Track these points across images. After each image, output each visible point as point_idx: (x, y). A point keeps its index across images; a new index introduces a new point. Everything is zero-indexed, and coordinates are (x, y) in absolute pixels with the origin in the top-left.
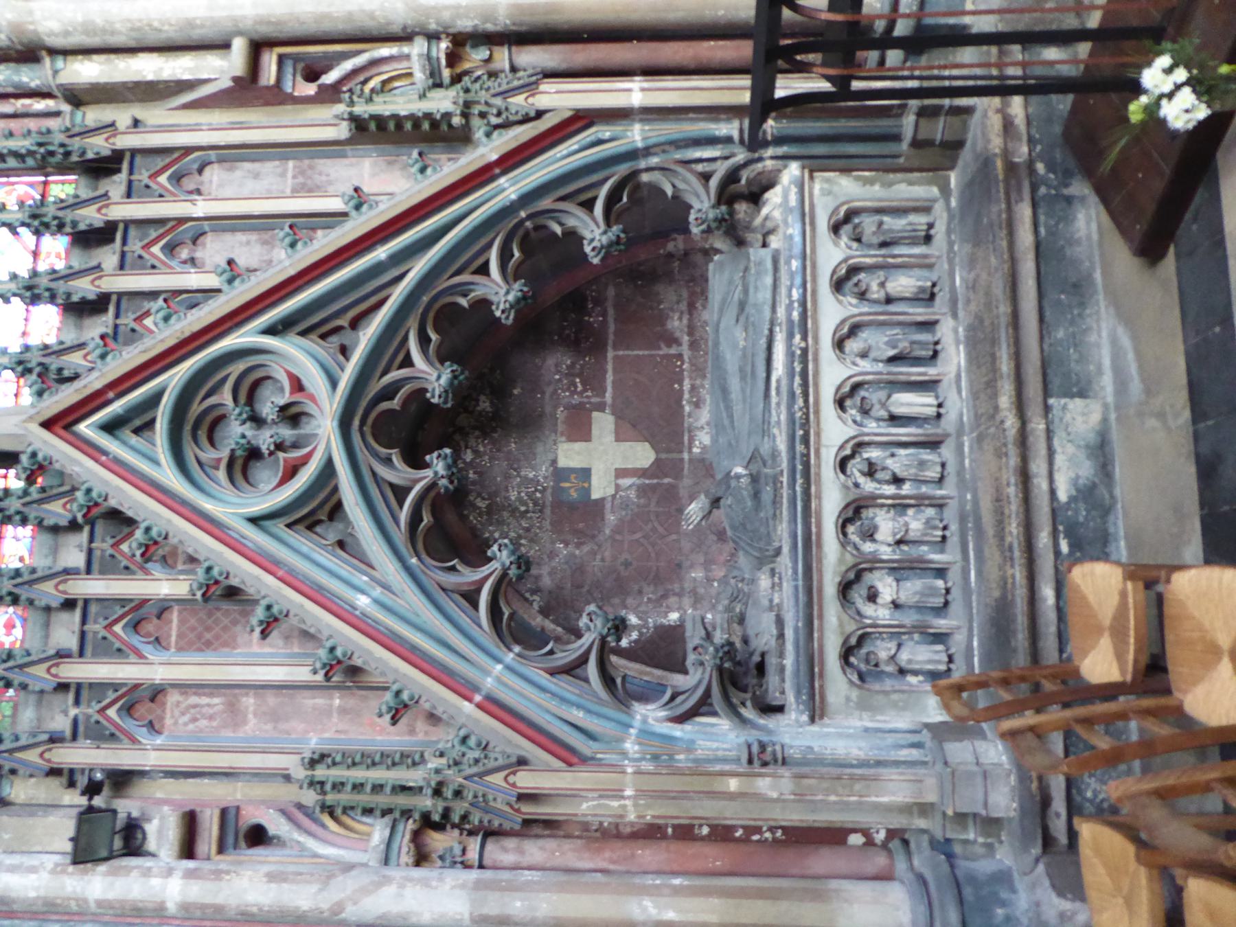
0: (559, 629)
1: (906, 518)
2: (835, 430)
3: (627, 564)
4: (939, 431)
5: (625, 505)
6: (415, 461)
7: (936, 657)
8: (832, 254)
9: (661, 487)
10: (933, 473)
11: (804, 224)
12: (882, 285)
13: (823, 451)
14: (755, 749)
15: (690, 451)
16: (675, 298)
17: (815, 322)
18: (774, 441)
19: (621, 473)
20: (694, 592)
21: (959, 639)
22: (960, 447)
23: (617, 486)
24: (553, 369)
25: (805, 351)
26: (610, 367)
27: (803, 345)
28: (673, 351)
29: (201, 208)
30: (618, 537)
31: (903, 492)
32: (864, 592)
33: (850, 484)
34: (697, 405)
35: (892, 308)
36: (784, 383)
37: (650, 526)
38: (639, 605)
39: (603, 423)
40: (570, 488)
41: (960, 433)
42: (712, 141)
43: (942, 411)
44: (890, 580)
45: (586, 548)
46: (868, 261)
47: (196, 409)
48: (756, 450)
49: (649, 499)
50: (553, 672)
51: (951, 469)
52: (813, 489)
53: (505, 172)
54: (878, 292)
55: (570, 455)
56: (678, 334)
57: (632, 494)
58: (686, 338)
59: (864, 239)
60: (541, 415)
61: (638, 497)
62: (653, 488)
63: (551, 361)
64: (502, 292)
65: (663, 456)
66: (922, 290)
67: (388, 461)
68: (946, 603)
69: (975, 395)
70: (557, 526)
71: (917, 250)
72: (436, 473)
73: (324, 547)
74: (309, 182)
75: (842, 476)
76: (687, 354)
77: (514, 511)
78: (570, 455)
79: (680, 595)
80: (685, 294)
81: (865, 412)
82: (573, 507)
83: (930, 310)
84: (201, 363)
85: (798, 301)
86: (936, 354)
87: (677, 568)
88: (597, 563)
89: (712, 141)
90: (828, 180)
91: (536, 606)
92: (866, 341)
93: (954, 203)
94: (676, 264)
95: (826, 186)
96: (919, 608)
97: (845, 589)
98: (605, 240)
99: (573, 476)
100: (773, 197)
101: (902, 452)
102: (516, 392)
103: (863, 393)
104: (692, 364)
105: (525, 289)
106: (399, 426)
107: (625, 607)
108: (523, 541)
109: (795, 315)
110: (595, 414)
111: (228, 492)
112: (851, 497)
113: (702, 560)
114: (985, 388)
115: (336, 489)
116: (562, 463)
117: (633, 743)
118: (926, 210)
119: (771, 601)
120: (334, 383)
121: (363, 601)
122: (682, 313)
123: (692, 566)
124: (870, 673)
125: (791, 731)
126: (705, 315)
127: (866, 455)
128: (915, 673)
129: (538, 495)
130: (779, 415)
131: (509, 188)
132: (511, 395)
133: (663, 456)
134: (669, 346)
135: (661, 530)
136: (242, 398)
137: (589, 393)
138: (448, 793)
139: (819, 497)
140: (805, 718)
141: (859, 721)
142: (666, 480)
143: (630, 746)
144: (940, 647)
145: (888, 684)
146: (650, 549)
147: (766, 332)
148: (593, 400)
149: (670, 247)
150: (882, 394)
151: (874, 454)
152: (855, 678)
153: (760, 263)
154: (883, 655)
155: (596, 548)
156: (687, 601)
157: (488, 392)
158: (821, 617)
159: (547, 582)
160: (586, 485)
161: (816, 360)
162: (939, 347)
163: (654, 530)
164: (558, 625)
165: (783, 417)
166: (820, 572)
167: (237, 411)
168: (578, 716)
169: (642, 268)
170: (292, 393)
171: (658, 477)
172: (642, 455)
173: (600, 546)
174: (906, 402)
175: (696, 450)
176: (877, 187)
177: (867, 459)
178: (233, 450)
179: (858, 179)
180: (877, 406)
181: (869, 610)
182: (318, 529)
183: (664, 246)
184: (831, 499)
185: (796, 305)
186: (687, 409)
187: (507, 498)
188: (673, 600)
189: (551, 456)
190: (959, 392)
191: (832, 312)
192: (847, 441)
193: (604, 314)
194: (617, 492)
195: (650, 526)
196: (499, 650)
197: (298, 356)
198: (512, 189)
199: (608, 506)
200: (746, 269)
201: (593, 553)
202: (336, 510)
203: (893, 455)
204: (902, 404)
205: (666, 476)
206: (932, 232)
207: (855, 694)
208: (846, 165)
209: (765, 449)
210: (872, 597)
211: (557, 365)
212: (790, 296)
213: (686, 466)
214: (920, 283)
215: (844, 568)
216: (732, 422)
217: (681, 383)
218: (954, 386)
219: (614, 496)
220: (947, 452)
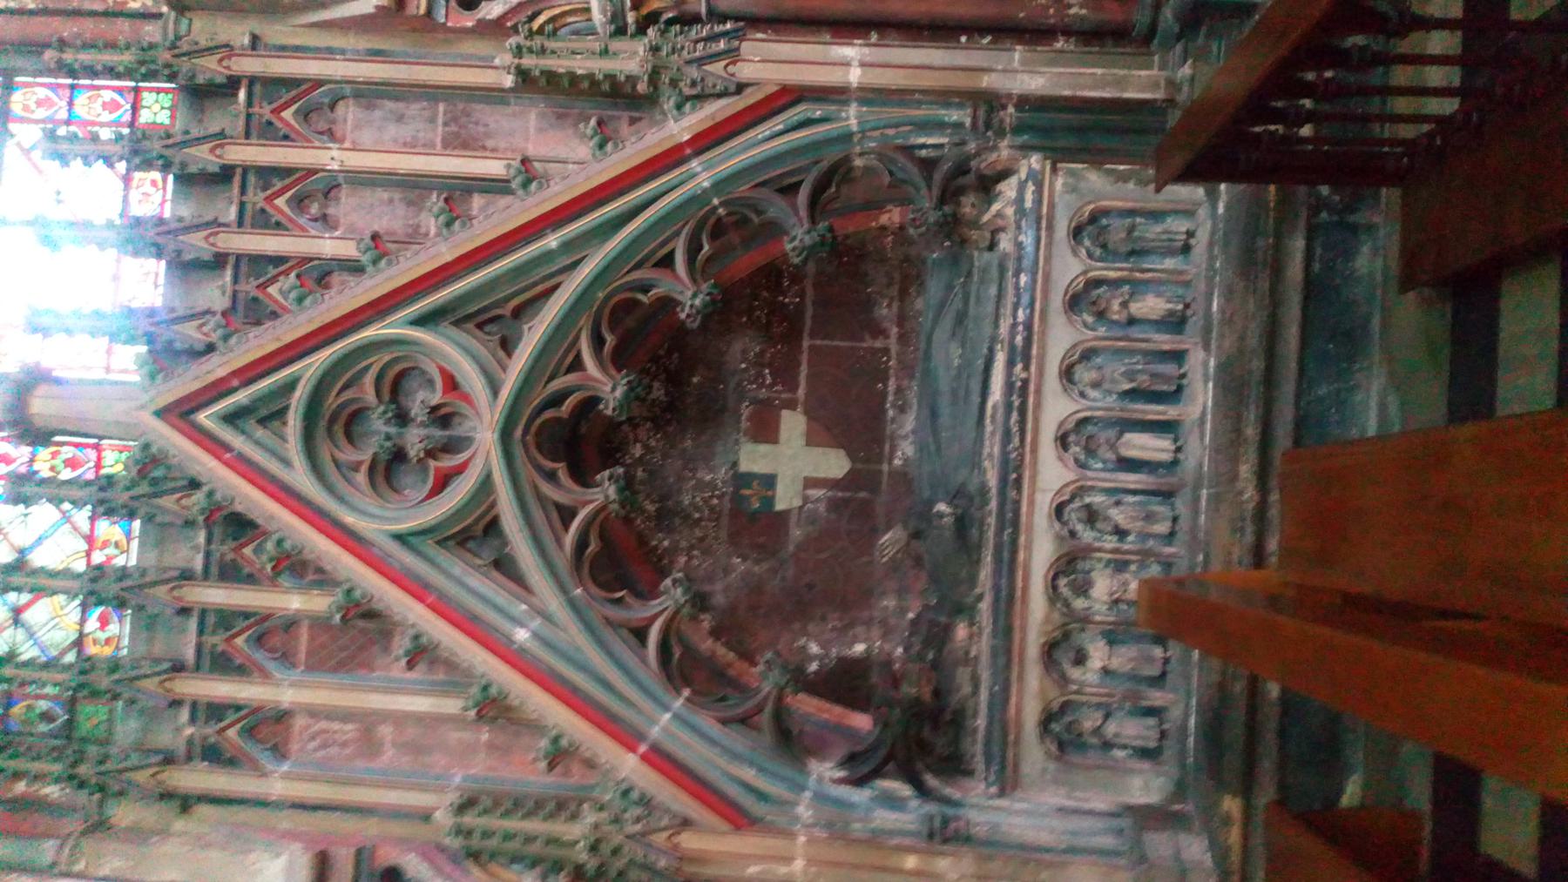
0: (731, 655)
1: (1127, 576)
2: (1052, 474)
3: (810, 586)
4: (1173, 480)
5: (812, 519)
6: (582, 476)
7: (1146, 733)
8: (1069, 268)
9: (855, 504)
10: (1162, 528)
11: (1039, 229)
12: (1124, 305)
13: (1039, 497)
14: (937, 823)
15: (890, 463)
16: (885, 281)
17: (1043, 348)
19: (810, 483)
20: (884, 623)
21: (1176, 713)
22: (1196, 500)
23: (806, 500)
24: (739, 356)
25: (1025, 382)
26: (804, 358)
27: (1024, 375)
28: (878, 344)
29: (331, 158)
31: (1126, 547)
32: (1072, 655)
33: (1065, 532)
34: (902, 410)
35: (1135, 332)
36: (1001, 411)
39: (793, 424)
41: (1197, 487)
42: (940, 126)
43: (1181, 456)
44: (1101, 644)
45: (765, 566)
46: (1112, 274)
47: (331, 402)
50: (724, 722)
51: (1184, 524)
52: (1022, 539)
53: (698, 153)
54: (1119, 312)
55: (754, 458)
56: (886, 324)
57: (822, 508)
59: (1110, 246)
60: (723, 410)
61: (828, 510)
62: (846, 502)
63: (737, 347)
64: (689, 293)
65: (859, 466)
66: (1171, 313)
67: (551, 476)
68: (1164, 674)
69: (1216, 450)
70: (734, 539)
71: (1170, 263)
72: (607, 497)
73: (477, 568)
74: (463, 131)
75: (1057, 525)
76: (894, 348)
77: (687, 517)
78: (754, 458)
79: (868, 623)
80: (897, 276)
81: (1090, 451)
82: (754, 516)
83: (1178, 338)
84: (339, 354)
85: (1024, 323)
86: (1180, 389)
89: (940, 126)
90: (1071, 173)
91: (706, 625)
92: (1100, 368)
93: (1221, 210)
95: (1070, 180)
96: (1134, 677)
97: (1050, 651)
98: (808, 240)
100: (1008, 189)
101: (1131, 499)
102: (695, 380)
103: (1090, 429)
104: (899, 362)
105: (715, 291)
106: (566, 438)
108: (695, 552)
109: (1019, 339)
111: (369, 502)
112: (1065, 550)
114: (1228, 447)
115: (493, 505)
116: (744, 467)
117: (808, 807)
118: (1189, 213)
119: (967, 653)
120: (495, 392)
121: (521, 635)
122: (892, 299)
123: (884, 593)
124: (1071, 743)
125: (979, 805)
126: (919, 304)
127: (1087, 500)
128: (1125, 747)
129: (715, 501)
131: (701, 174)
132: (689, 384)
133: (859, 466)
136: (386, 397)
137: (779, 388)
138: (606, 849)
139: (1029, 547)
140: (993, 790)
141: (1055, 798)
142: (862, 495)
143: (804, 811)
144: (1151, 721)
145: (1093, 757)
147: (985, 351)
148: (784, 396)
149: (884, 219)
150: (1111, 433)
151: (1097, 499)
152: (1053, 748)
153: (985, 270)
154: (1088, 725)
156: (876, 632)
157: (663, 377)
158: (1021, 678)
159: (719, 600)
161: (1038, 392)
162: (1185, 382)
164: (731, 649)
165: (996, 450)
166: (1024, 629)
167: (382, 408)
168: (749, 774)
170: (445, 392)
172: (835, 464)
175: (897, 462)
176: (1131, 185)
178: (375, 454)
179: (1110, 172)
181: (1075, 673)
182: (471, 544)
183: (876, 219)
184: (1041, 551)
185: (1020, 328)
186: (891, 413)
187: (679, 503)
188: (860, 630)
189: (732, 458)
190: (1202, 438)
191: (1061, 337)
192: (1067, 485)
196: (666, 697)
197: (450, 350)
198: (704, 175)
199: (793, 519)
200: (969, 274)
201: (774, 571)
202: (492, 527)
203: (1118, 503)
204: (1134, 446)
206: (1192, 242)
207: (1052, 766)
208: (1096, 157)
209: (972, 487)
210: (1080, 659)
211: (744, 352)
212: (1015, 317)
214: (1170, 306)
215: (1050, 628)
217: (885, 381)
218: (1196, 430)
219: (801, 508)
220: (1181, 505)
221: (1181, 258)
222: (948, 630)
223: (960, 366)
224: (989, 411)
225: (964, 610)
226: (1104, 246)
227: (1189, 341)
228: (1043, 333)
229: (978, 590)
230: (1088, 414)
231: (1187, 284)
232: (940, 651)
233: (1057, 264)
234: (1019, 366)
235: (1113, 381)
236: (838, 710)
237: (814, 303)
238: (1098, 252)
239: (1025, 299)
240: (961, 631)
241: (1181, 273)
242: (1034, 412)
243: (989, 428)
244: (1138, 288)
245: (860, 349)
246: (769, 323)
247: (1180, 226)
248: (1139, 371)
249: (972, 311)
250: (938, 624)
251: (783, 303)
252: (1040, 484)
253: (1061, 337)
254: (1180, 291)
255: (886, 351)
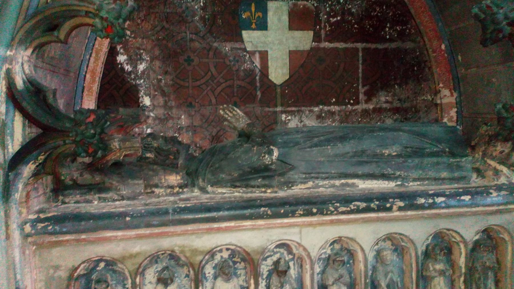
3: (189, 61)
5: (239, 59)
13: (296, 230)
15: (282, 112)
16: (403, 97)
18: (301, 183)
19: (264, 56)
20: (168, 118)
23: (252, 53)
26: (349, 45)
30: (211, 53)
34: (319, 117)
37: (222, 81)
38: (154, 72)
39: (303, 40)
40: (251, 12)
45: (200, 25)
48: (293, 168)
49: (243, 80)
54: (435, 270)
56: (374, 100)
57: (247, 66)
58: (371, 107)
61: (245, 70)
62: (252, 82)
65: (279, 90)
75: (274, 246)
76: (362, 106)
79: (165, 106)
80: (406, 105)
87: (187, 104)
88: (189, 36)
94: (429, 97)
99: (260, 14)
107: (152, 60)
110: (311, 33)
112: (255, 257)
113: (195, 124)
123: (190, 115)
130: (325, 187)
133: (279, 90)
134: (365, 93)
135: (220, 89)
142: (259, 93)
146: (203, 81)
148: (323, 32)
151: (293, 272)
153: (459, 167)
155: (202, 34)
156: (161, 112)
160: (254, 26)
163: (219, 84)
169: (427, 70)
171: (261, 86)
172: (278, 73)
173: (203, 38)
175: (284, 116)
177: (289, 267)
185: (431, 201)
186: (316, 109)
188: (161, 100)
192: (305, 249)
193: (391, 40)
194: (248, 52)
195: (222, 81)
199: (237, 45)
200: (453, 155)
205: (263, 93)
209: (293, 175)
212: (438, 195)
213: (271, 109)
216: (316, 145)
219: (245, 50)
222: (173, 168)
223: (383, 155)
224: (350, 181)
225: (192, 178)
228: (422, 217)
229: (209, 189)
232: (155, 163)
233: (469, 221)
234: (402, 204)
236: (96, 87)
237: (386, 49)
239: (452, 202)
240: (174, 179)
242: (363, 219)
243: (337, 183)
245: (358, 85)
246: (371, 18)
249: (427, 160)
250: (176, 158)
251: (386, 27)
252: (305, 230)
255: (357, 102)
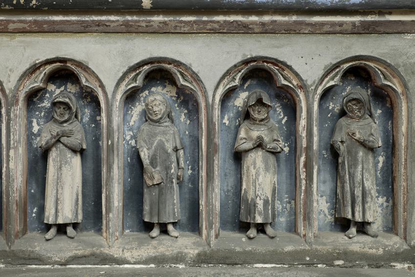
4: (16, 226)
12: (260, 145)
35: (222, 161)
59: (343, 121)
66: (251, 208)
71: (321, 206)
83: (217, 224)
118: (391, 227)
150: (78, 135)
174: (67, 180)
180: (56, 129)
214: (260, 204)
218: (88, 251)
221: (330, 219)
226: (343, 113)
227: (215, 235)
230: (103, 105)
231: (293, 228)
235: (152, 136)
238: (334, 106)
241: (307, 218)
244: (287, 159)
247: (375, 211)
248: (167, 168)
253: (209, 57)
254: (282, 220)
